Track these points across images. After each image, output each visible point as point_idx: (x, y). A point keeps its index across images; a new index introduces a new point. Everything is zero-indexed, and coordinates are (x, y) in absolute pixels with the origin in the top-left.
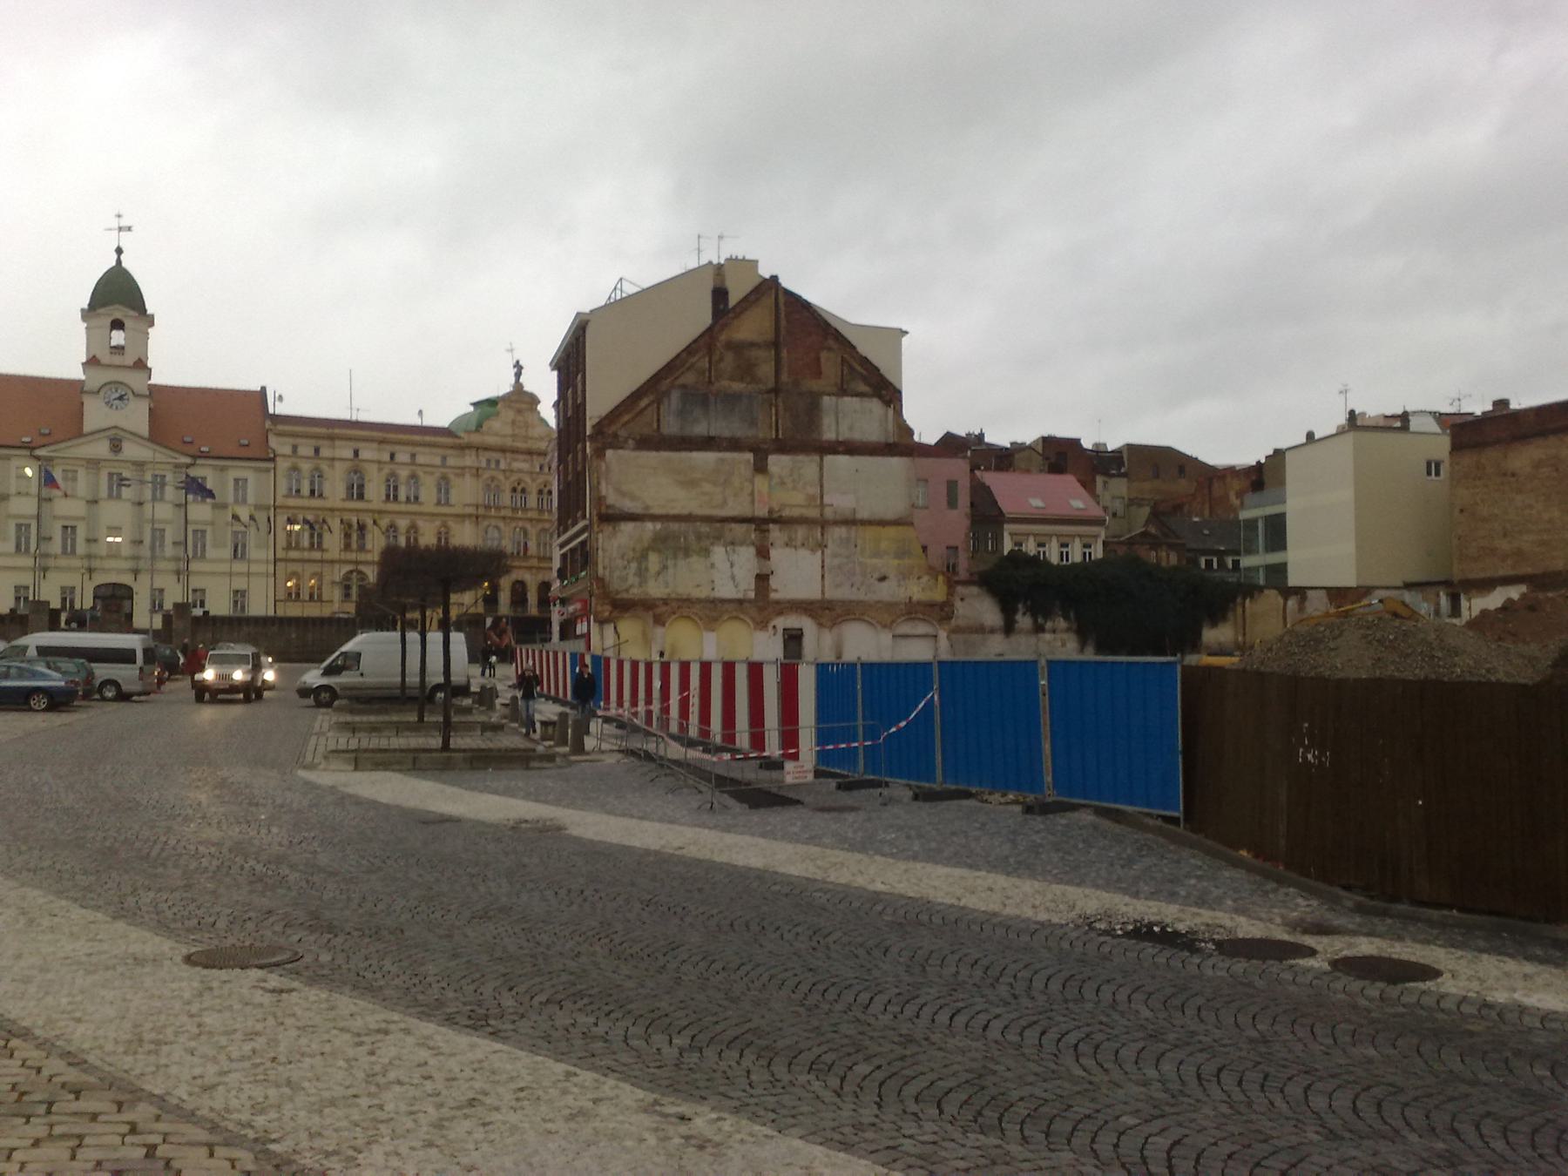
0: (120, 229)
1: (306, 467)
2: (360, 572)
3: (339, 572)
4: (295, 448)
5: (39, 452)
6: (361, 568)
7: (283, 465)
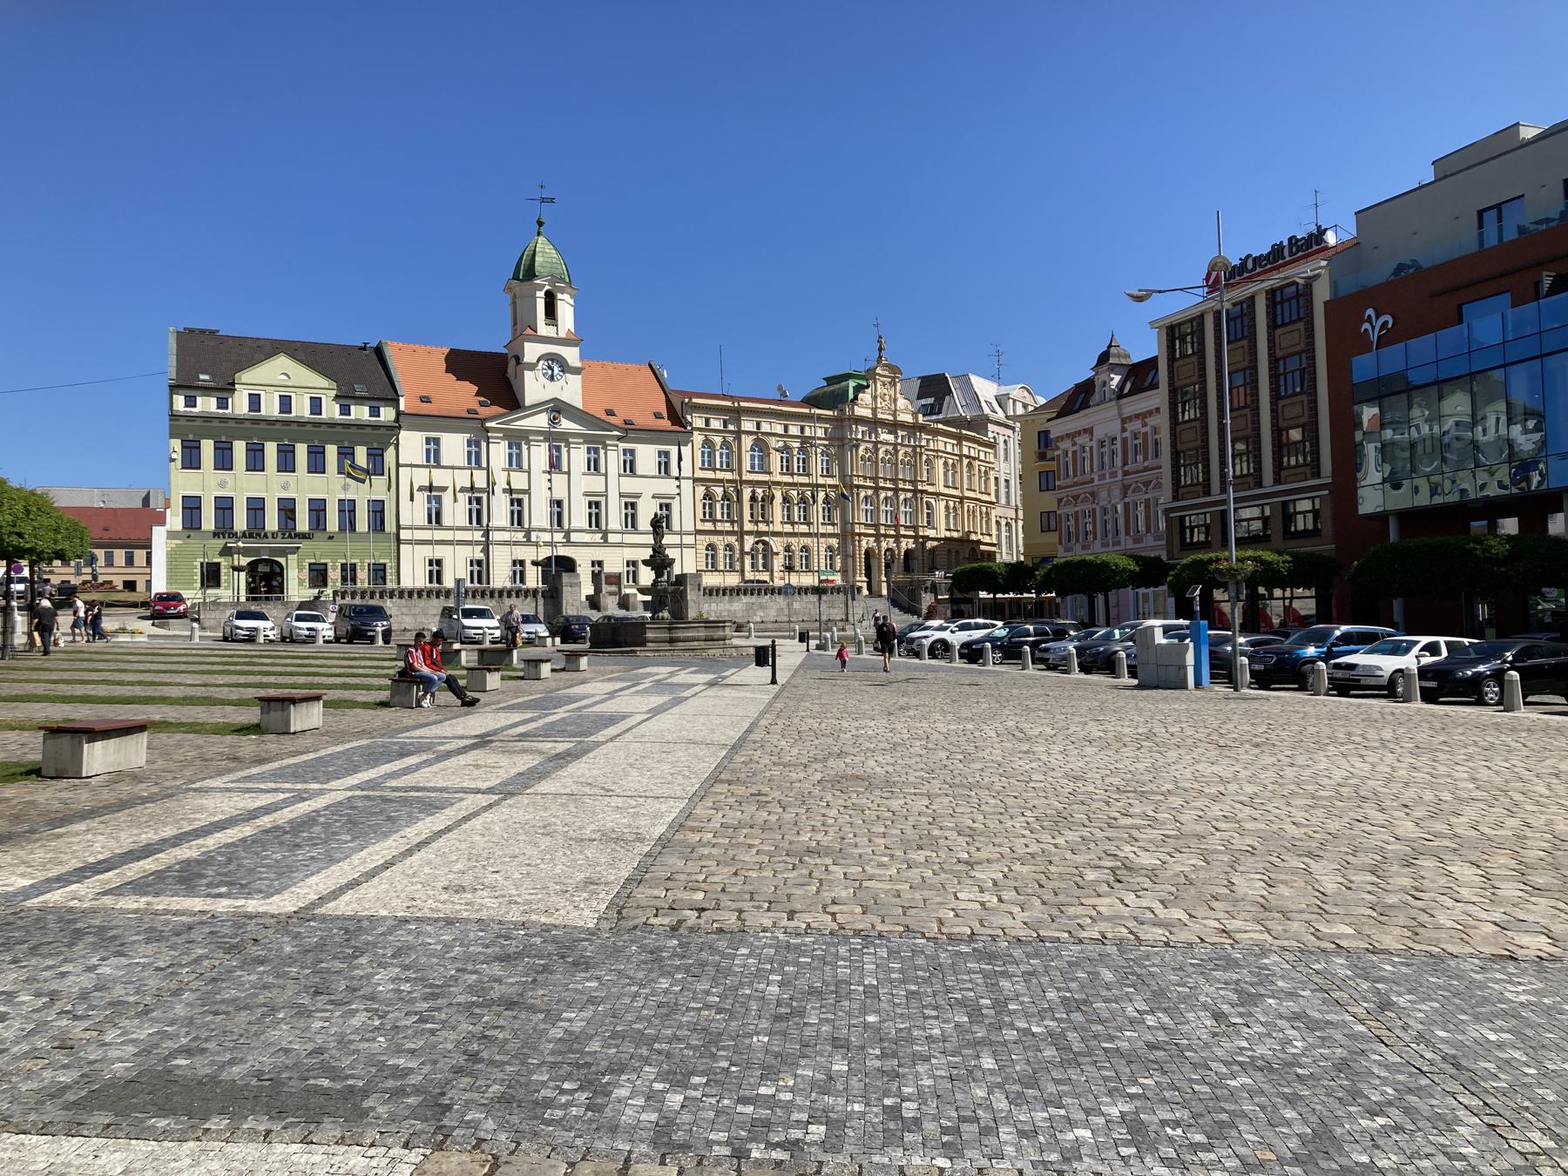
0: (543, 200)
1: (718, 440)
2: (765, 543)
3: (749, 541)
4: (707, 422)
5: (488, 425)
6: (766, 539)
7: (698, 438)
